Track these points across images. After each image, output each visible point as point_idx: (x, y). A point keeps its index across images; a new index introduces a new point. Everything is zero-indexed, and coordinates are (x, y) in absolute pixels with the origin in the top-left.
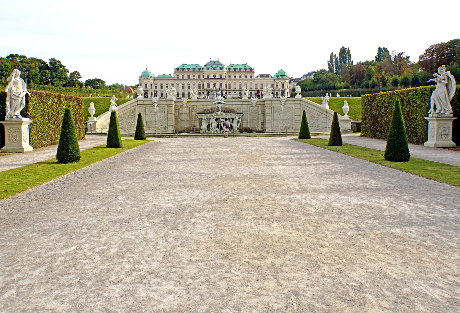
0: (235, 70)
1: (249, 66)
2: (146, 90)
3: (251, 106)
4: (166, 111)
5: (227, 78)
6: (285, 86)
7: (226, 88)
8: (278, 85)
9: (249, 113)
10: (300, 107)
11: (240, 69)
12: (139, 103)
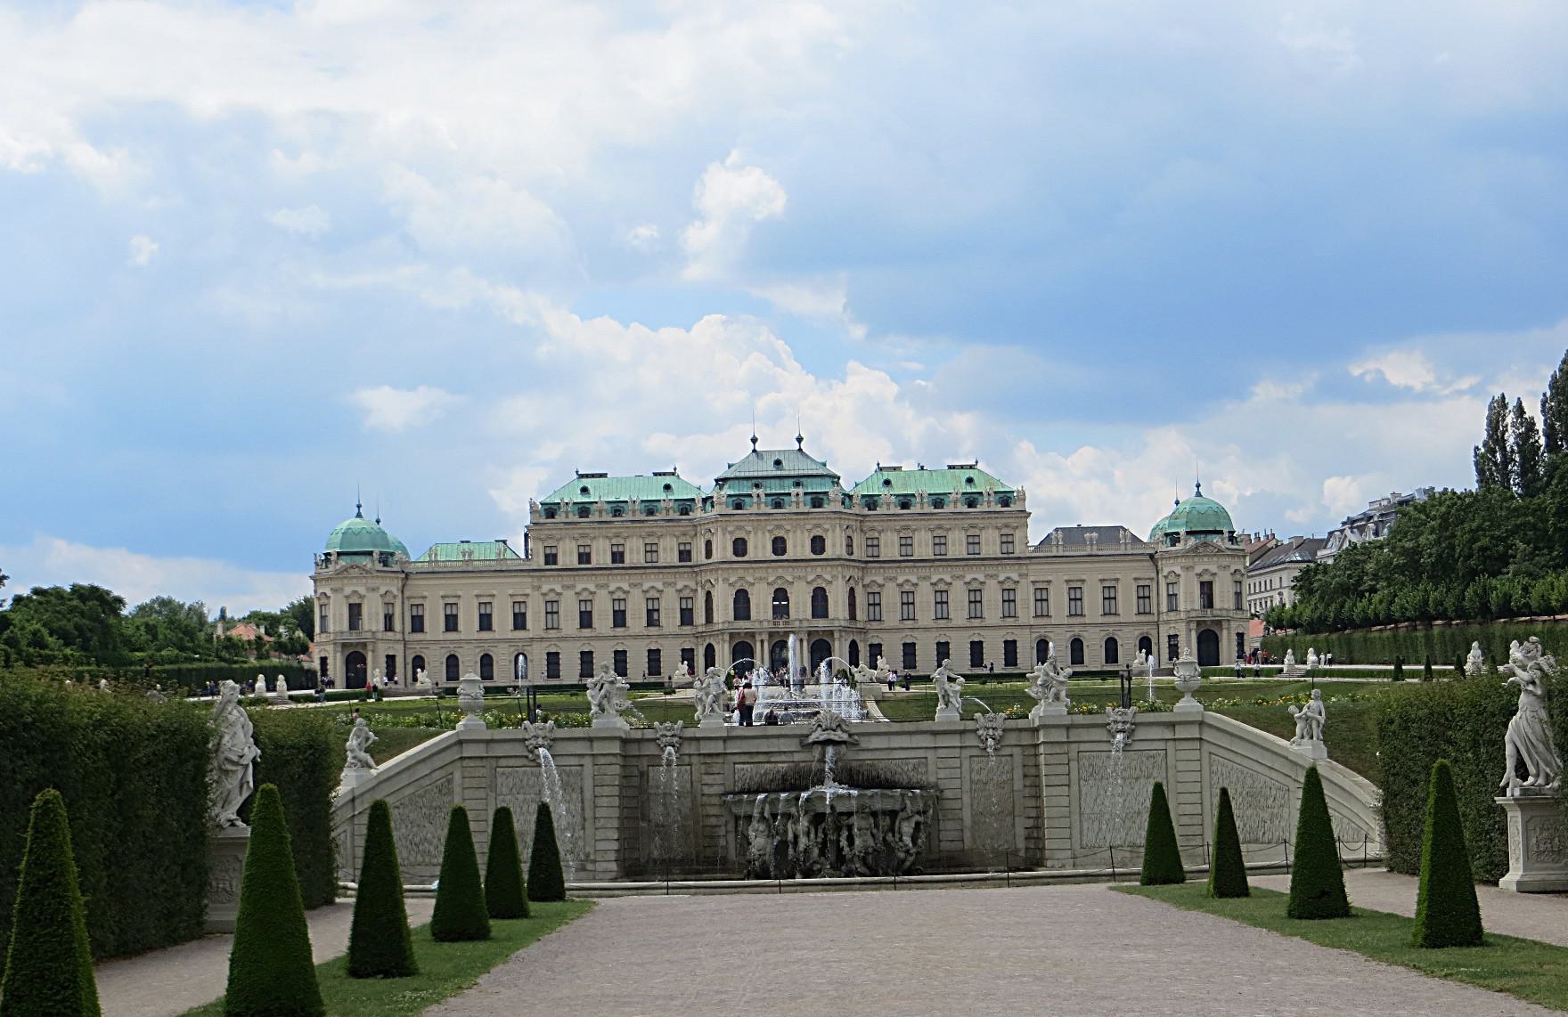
0: (905, 505)
2: (353, 638)
3: (975, 752)
4: (588, 784)
6: (1223, 598)
8: (1181, 590)
9: (967, 787)
10: (1196, 755)
11: (938, 501)
12: (469, 751)
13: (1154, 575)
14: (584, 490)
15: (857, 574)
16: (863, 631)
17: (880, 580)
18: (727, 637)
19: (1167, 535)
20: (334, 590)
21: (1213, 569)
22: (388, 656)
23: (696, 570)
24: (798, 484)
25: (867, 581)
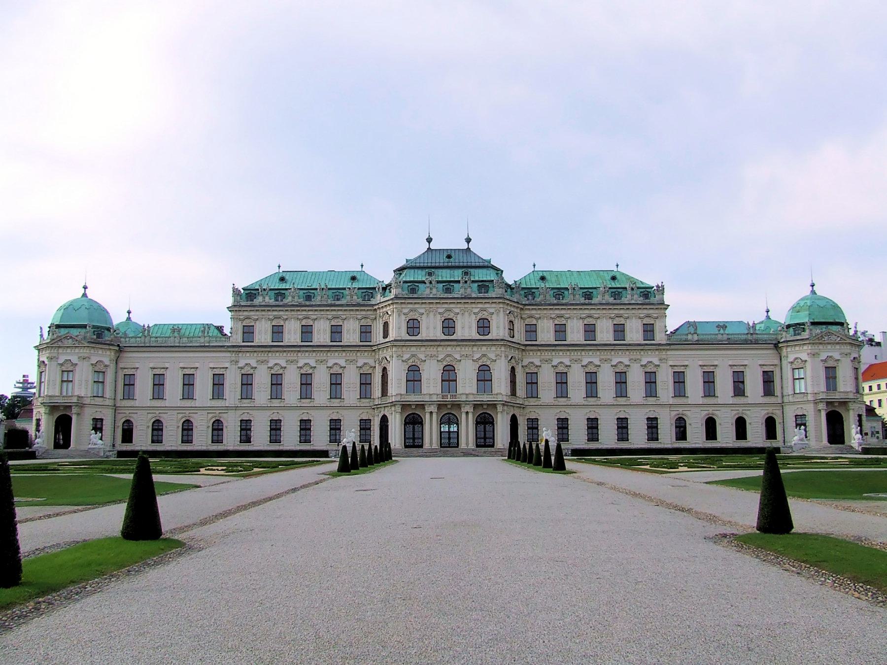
1: (629, 278)
5: (520, 336)
6: (845, 384)
7: (513, 392)
11: (588, 294)
13: (777, 362)
14: (282, 279)
15: (516, 354)
16: (522, 407)
17: (538, 363)
18: (399, 409)
19: (788, 326)
20: (51, 359)
21: (836, 356)
22: (95, 420)
23: (373, 349)
24: (466, 273)
25: (525, 362)
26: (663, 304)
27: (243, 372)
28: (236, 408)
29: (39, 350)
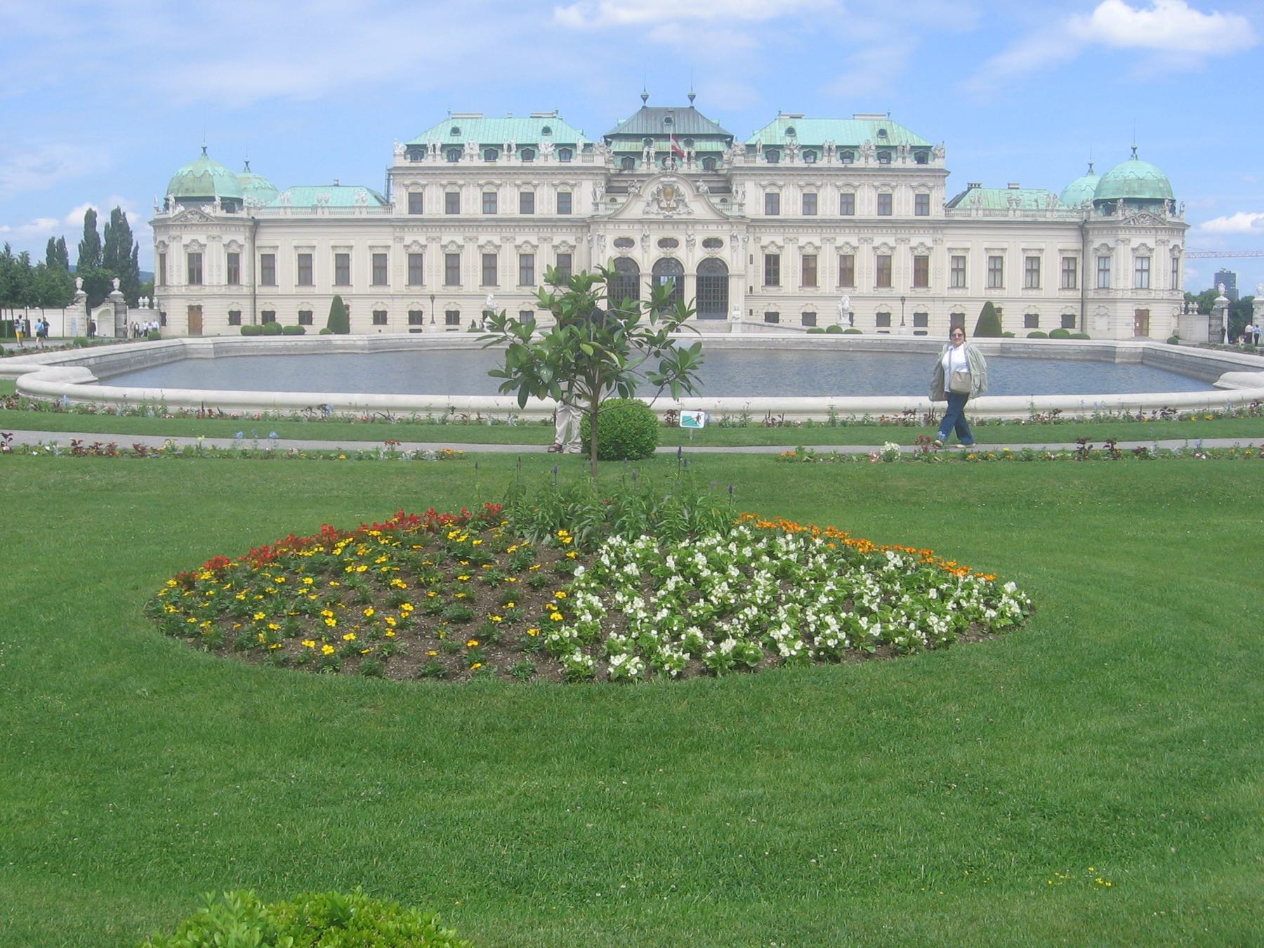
11: (847, 153)
13: (1079, 246)
14: (456, 131)
17: (779, 241)
19: (1097, 203)
21: (1151, 243)
22: (231, 313)
26: (941, 170)
27: (411, 251)
28: (403, 296)
29: (155, 227)
